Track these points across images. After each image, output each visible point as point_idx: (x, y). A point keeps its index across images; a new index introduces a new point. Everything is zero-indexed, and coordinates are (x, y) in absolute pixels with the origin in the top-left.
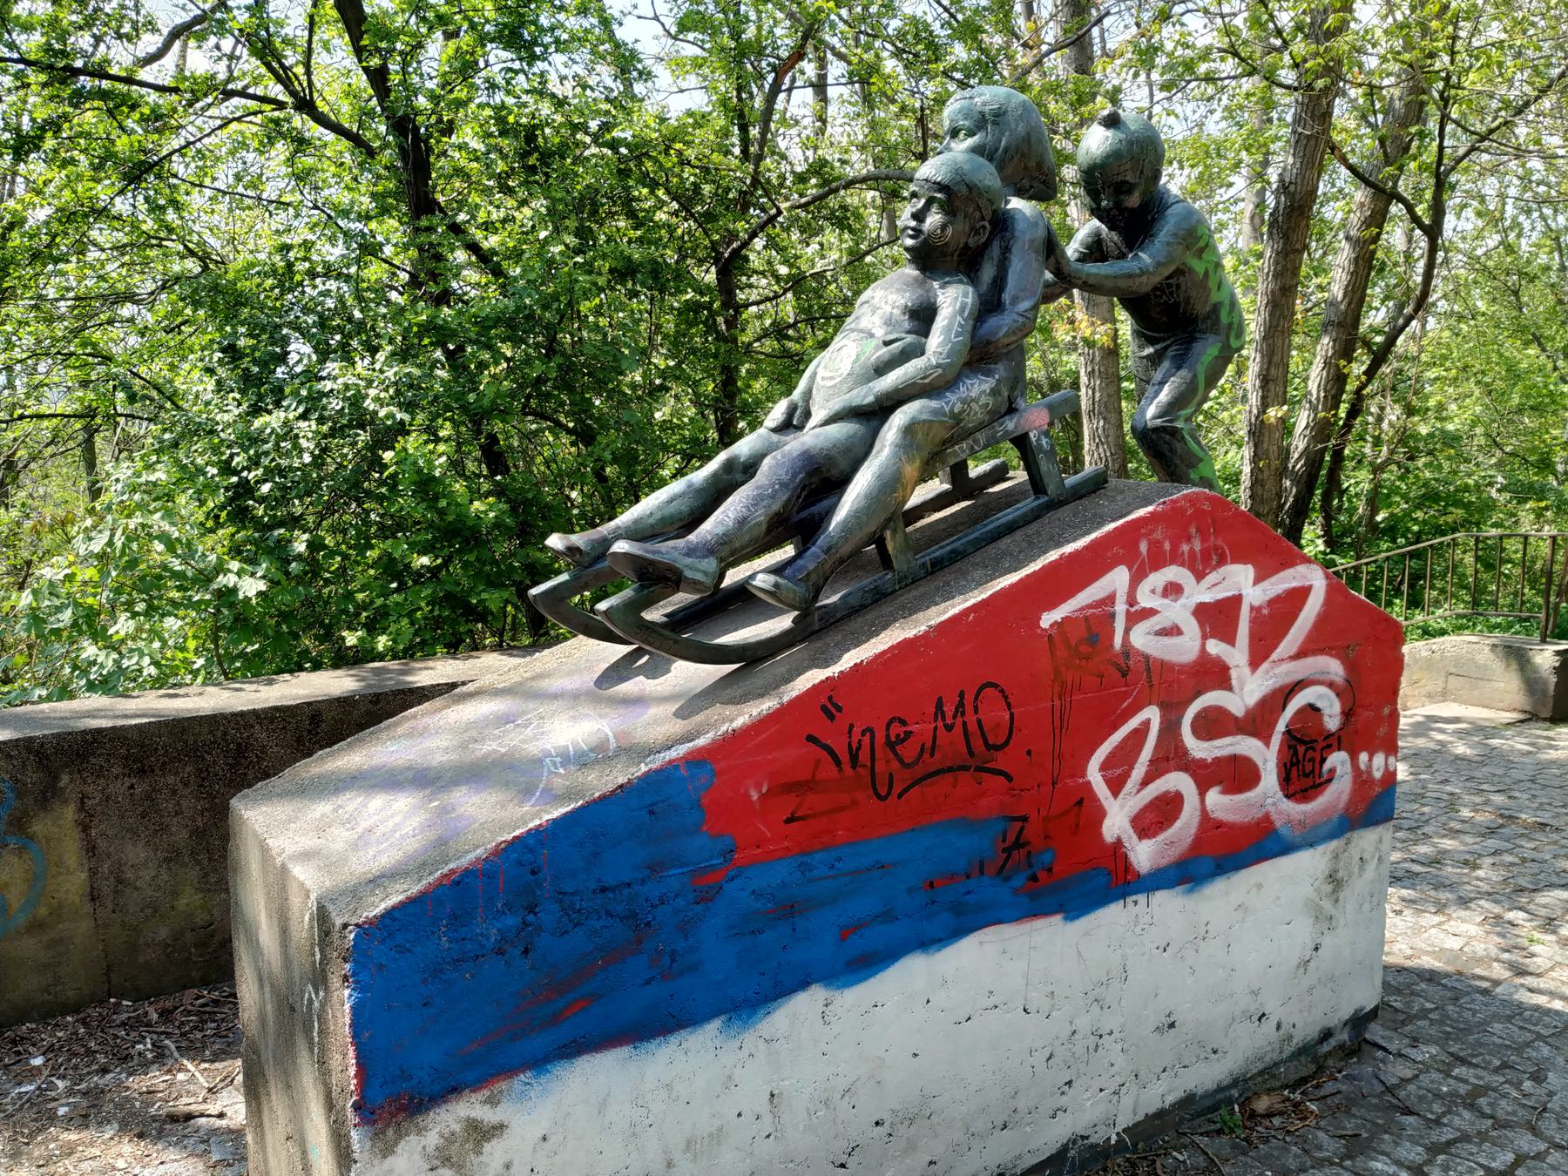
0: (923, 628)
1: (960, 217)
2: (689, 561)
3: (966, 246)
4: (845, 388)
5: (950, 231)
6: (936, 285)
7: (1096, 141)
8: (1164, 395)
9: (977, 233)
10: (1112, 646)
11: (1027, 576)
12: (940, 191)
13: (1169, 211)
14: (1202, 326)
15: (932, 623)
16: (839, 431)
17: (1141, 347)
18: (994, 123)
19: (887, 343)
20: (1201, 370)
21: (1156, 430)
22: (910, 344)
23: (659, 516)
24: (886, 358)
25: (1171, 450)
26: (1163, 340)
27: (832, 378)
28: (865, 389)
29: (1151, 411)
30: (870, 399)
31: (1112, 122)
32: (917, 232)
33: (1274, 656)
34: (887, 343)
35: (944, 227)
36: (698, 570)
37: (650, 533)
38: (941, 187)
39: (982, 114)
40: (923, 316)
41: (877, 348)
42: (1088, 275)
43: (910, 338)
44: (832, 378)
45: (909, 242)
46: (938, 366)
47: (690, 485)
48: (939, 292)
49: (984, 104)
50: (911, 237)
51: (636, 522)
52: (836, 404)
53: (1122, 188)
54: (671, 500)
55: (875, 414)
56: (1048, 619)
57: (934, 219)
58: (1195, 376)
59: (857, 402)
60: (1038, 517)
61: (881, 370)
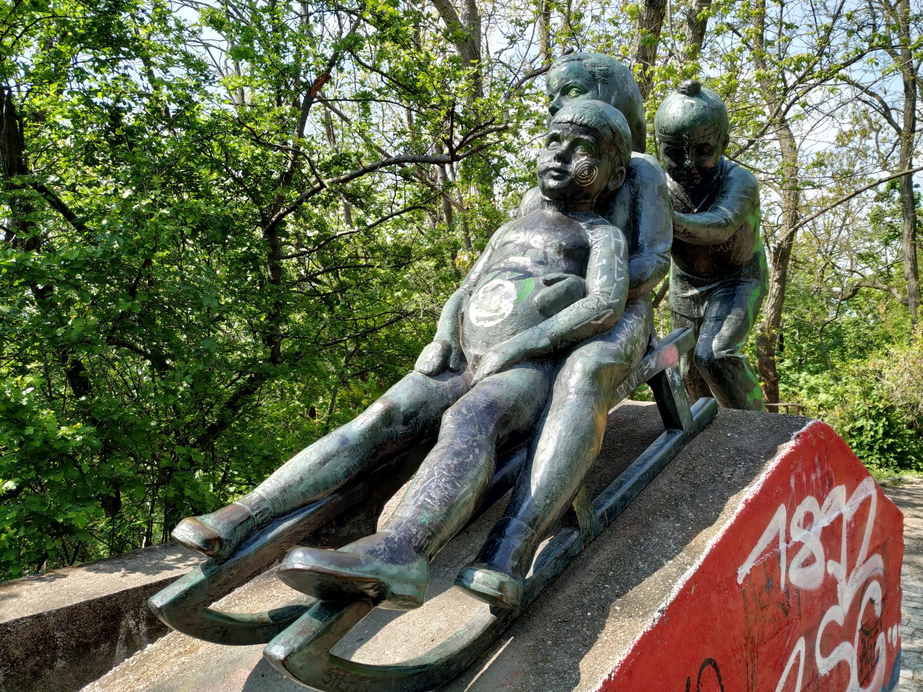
0: (657, 615)
1: (605, 163)
2: (394, 569)
3: (606, 189)
4: (509, 329)
5: (595, 173)
6: (583, 225)
7: (675, 108)
8: (726, 330)
9: (616, 178)
10: (779, 588)
11: (754, 543)
12: (586, 133)
13: (731, 174)
14: (745, 271)
15: (663, 605)
16: (519, 378)
17: (685, 289)
18: (604, 82)
19: (548, 283)
20: (750, 307)
21: (722, 360)
22: (572, 284)
23: (311, 481)
24: (552, 297)
25: (733, 377)
26: (710, 284)
27: (491, 319)
28: (536, 330)
29: (715, 344)
30: (544, 342)
31: (694, 91)
32: (562, 173)
33: (858, 564)
34: (548, 283)
35: (591, 168)
36: (407, 582)
37: (300, 502)
38: (586, 128)
39: (593, 74)
40: (577, 257)
41: (538, 288)
42: (689, 223)
43: (571, 278)
44: (491, 319)
45: (552, 183)
46: (609, 306)
47: (344, 441)
48: (589, 232)
49: (593, 65)
50: (555, 178)
51: (284, 491)
52: (511, 345)
53: (702, 150)
54: (324, 461)
55: (550, 358)
56: (744, 570)
57: (580, 162)
58: (746, 314)
59: (532, 344)
60: (678, 452)
61: (548, 310)
